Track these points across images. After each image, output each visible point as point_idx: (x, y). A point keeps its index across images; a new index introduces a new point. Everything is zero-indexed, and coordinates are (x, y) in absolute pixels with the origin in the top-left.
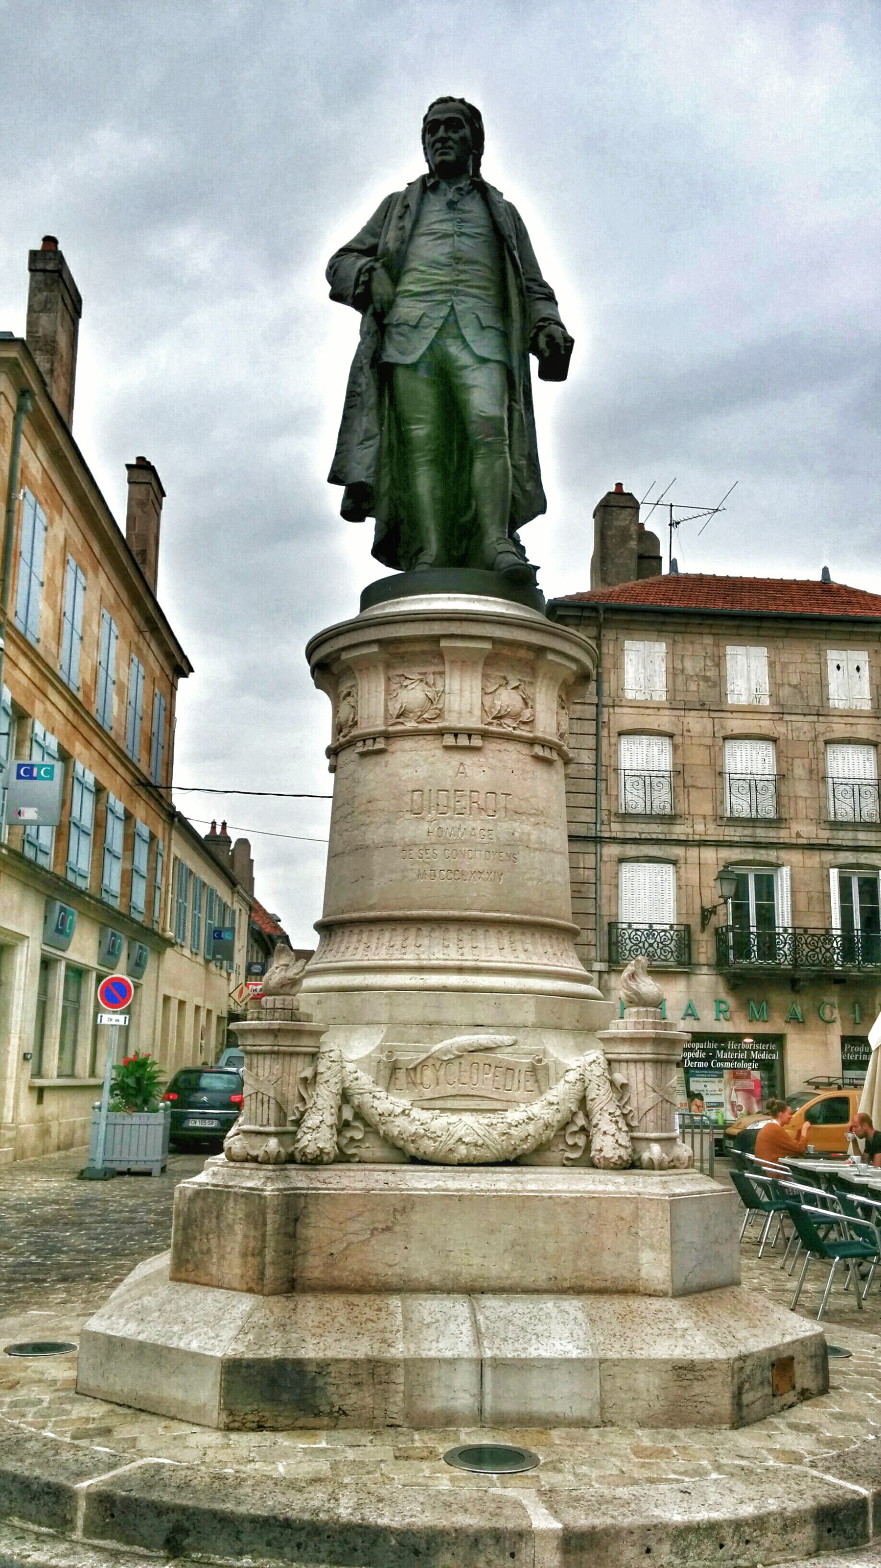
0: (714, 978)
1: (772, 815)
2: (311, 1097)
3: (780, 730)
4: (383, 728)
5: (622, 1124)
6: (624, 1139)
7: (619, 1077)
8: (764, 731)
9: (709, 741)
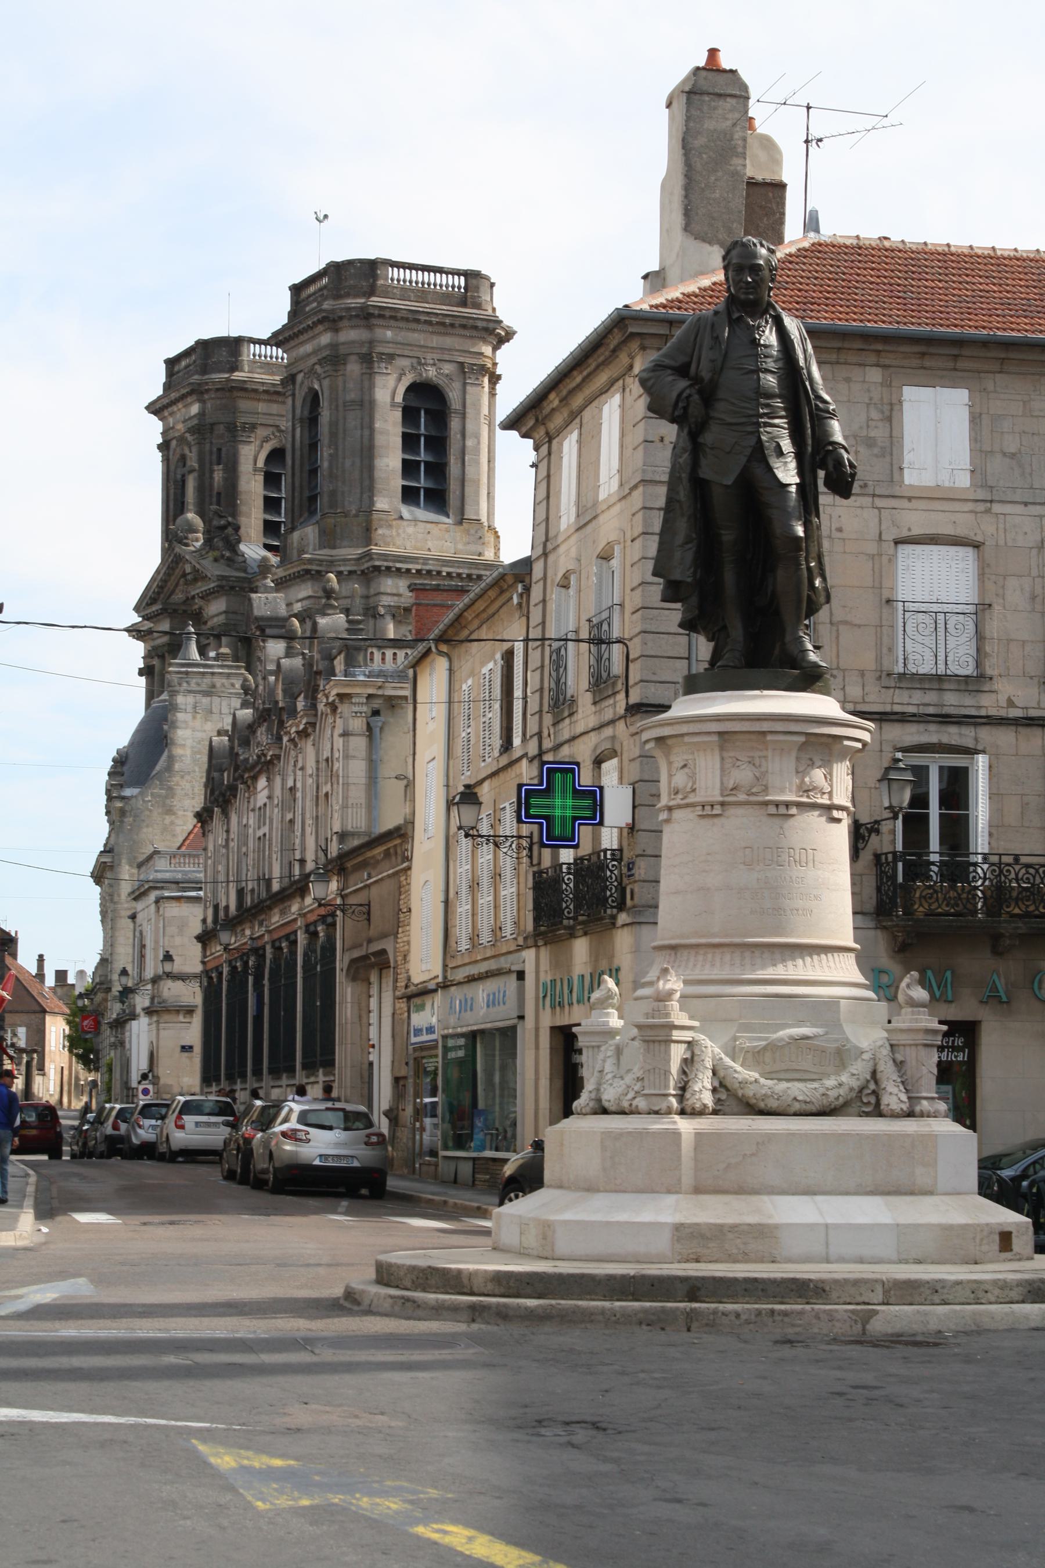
0: (872, 933)
1: (969, 670)
2: (692, 1071)
3: (986, 529)
4: (721, 799)
5: (902, 1088)
6: (904, 1097)
7: (899, 1057)
8: (961, 531)
9: (872, 548)
